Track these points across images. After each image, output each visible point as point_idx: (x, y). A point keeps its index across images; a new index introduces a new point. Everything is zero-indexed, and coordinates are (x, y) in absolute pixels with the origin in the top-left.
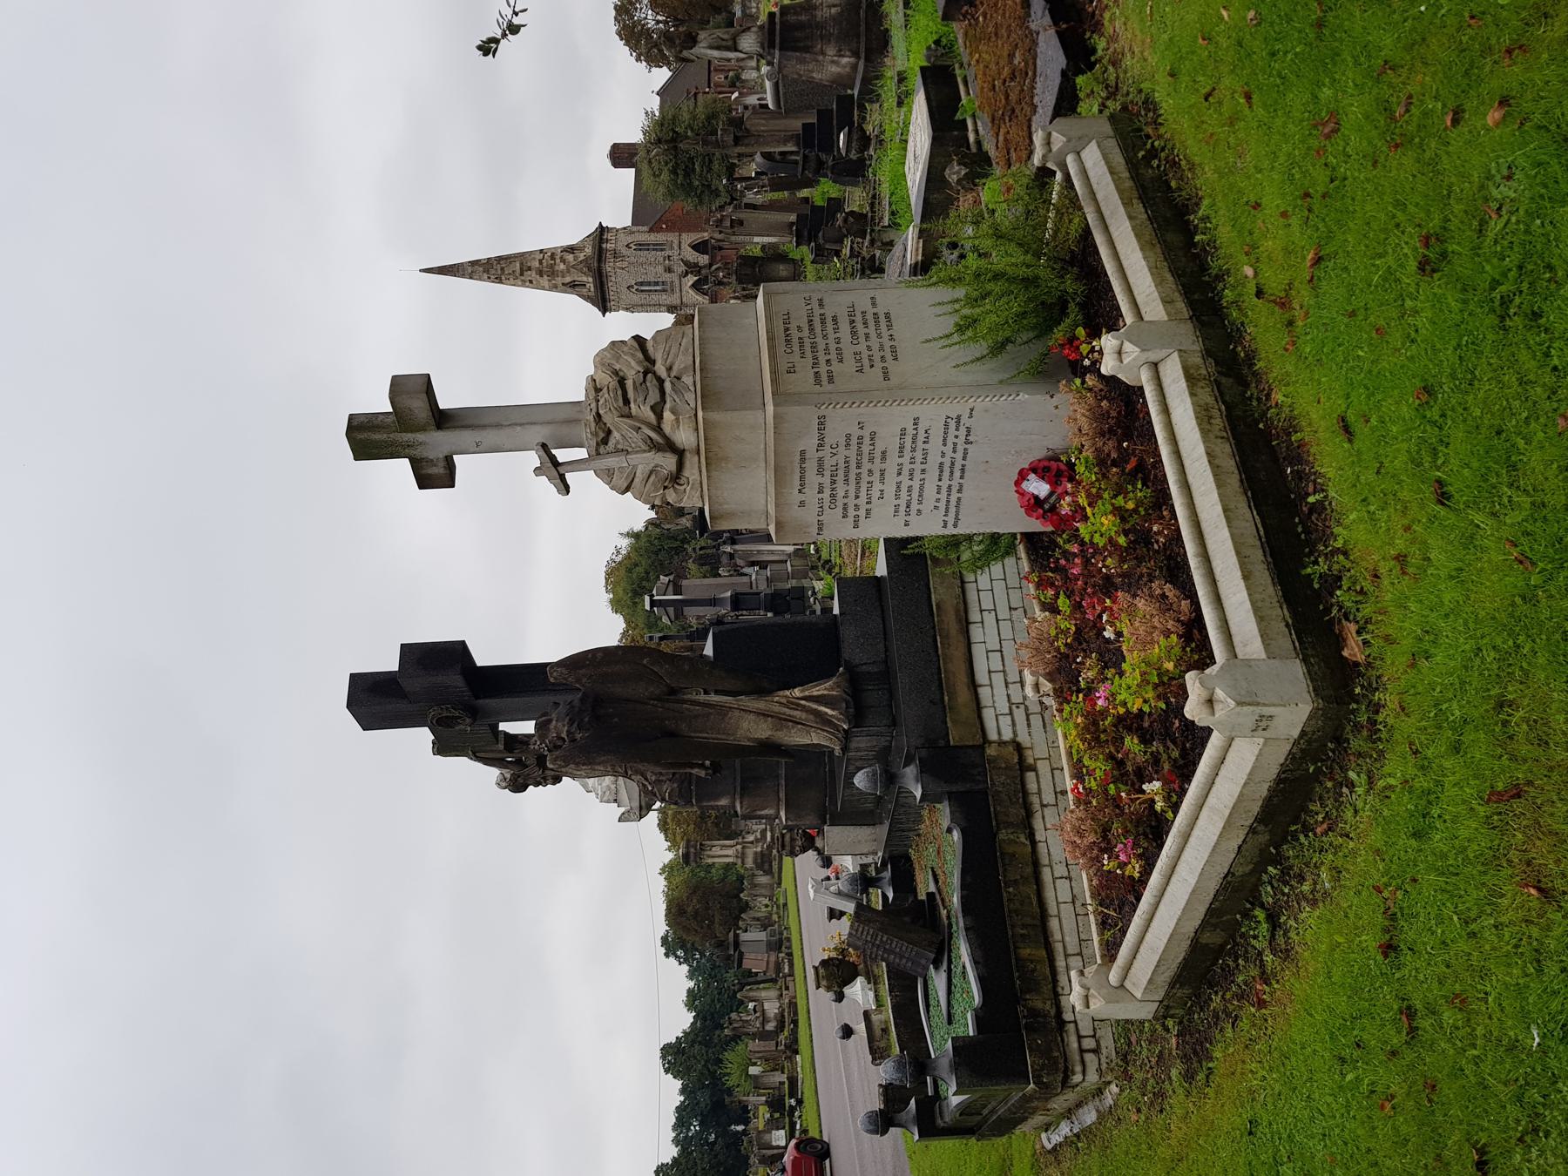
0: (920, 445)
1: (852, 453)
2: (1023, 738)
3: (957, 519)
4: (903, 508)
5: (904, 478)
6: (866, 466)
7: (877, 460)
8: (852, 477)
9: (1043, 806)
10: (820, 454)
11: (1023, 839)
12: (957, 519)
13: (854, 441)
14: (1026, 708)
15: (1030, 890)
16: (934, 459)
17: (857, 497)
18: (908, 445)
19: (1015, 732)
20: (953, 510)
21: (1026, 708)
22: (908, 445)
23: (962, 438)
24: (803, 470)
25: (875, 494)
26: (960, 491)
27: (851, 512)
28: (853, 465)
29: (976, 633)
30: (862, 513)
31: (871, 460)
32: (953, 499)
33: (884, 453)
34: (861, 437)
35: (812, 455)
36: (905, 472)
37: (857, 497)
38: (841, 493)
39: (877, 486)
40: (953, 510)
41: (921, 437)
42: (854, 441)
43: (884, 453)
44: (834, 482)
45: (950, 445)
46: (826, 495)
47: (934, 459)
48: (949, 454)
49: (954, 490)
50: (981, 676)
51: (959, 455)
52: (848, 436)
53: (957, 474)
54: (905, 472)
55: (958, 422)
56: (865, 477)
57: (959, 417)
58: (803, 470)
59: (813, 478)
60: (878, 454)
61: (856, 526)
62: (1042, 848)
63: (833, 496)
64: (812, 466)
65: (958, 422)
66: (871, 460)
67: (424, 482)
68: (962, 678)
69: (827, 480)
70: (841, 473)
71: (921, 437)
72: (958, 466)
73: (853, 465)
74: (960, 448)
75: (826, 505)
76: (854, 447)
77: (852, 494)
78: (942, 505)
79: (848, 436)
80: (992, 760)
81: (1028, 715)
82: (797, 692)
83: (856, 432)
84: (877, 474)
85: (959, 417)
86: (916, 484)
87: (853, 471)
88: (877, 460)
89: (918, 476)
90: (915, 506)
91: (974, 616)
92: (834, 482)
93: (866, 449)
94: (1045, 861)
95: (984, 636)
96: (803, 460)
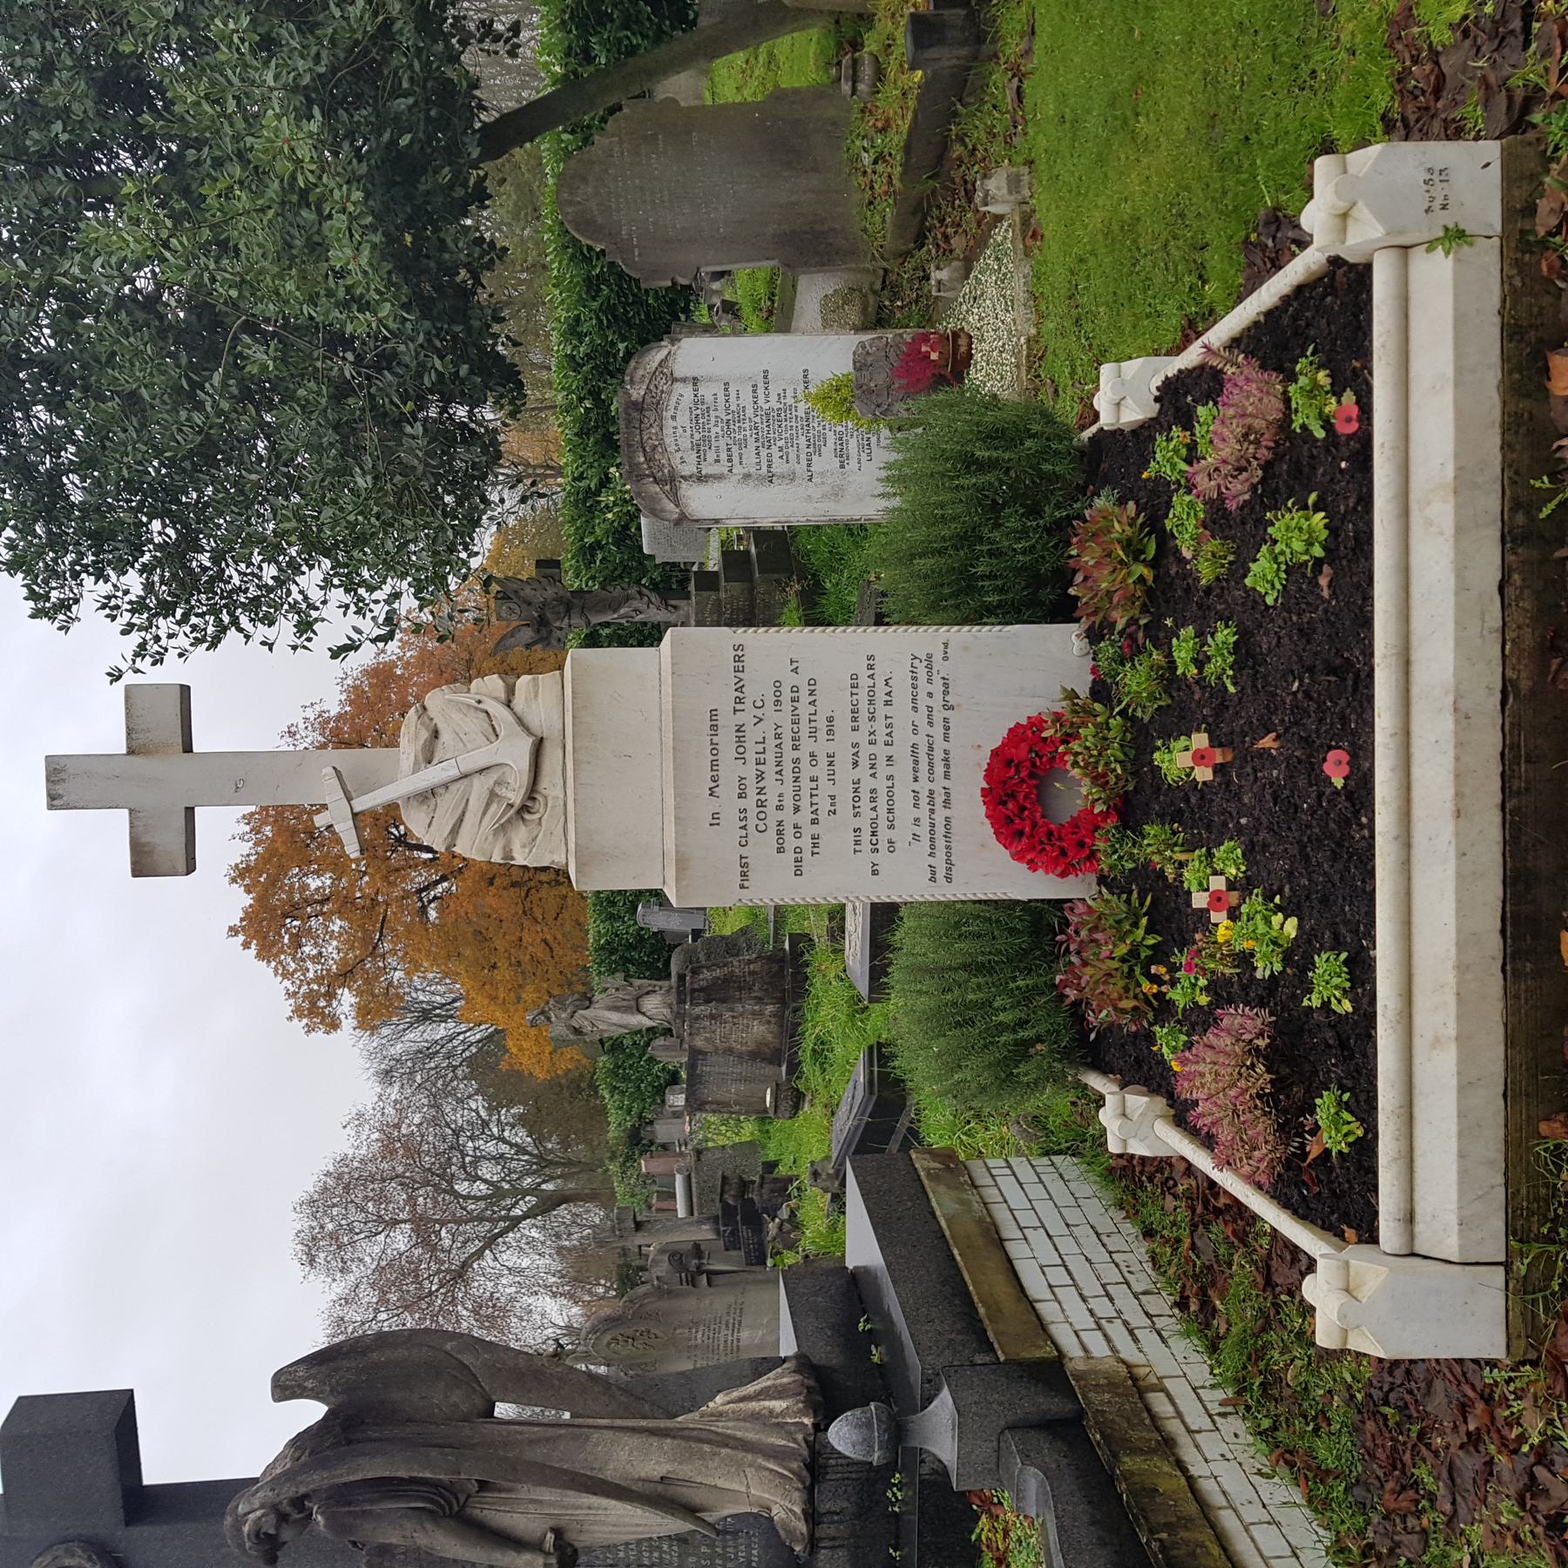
0: (882, 711)
1: (785, 719)
2: (1128, 1351)
3: (950, 864)
4: (866, 836)
5: (863, 772)
6: (807, 745)
7: (822, 735)
8: (788, 766)
9: (1189, 1431)
10: (740, 718)
11: (1166, 1468)
12: (950, 864)
13: (787, 695)
14: (1126, 1323)
15: (1205, 1536)
16: (904, 739)
17: (797, 809)
18: (864, 707)
19: (1113, 1349)
20: (941, 843)
21: (1126, 1323)
22: (864, 707)
23: (938, 696)
24: (714, 747)
25: (824, 805)
26: (947, 803)
27: (790, 842)
28: (787, 743)
29: (1016, 1250)
30: (806, 843)
31: (813, 734)
32: (938, 755)
33: (830, 720)
34: (795, 689)
35: (728, 721)
36: (864, 761)
37: (797, 809)
38: (772, 802)
39: (825, 787)
40: (941, 843)
41: (881, 697)
42: (787, 695)
43: (830, 720)
44: (760, 776)
45: (923, 710)
46: (750, 803)
47: (904, 739)
48: (924, 728)
49: (939, 800)
50: (1035, 1285)
51: (938, 731)
52: (778, 684)
53: (939, 769)
54: (864, 761)
55: (929, 667)
56: (807, 771)
57: (929, 656)
58: (714, 747)
59: (730, 770)
60: (822, 724)
61: (798, 873)
62: (1208, 1487)
63: (761, 804)
64: (727, 739)
65: (929, 667)
66: (813, 734)
67: (143, 864)
68: (1003, 1290)
69: (750, 771)
70: (770, 757)
71: (881, 697)
72: (938, 755)
73: (787, 743)
74: (938, 717)
75: (752, 822)
76: (787, 706)
77: (789, 803)
78: (924, 830)
79: (778, 684)
80: (1079, 1376)
81: (1131, 1332)
82: (719, 1399)
83: (789, 680)
84: (823, 761)
85: (929, 656)
86: (881, 785)
87: (788, 755)
88: (822, 735)
89: (883, 769)
90: (884, 834)
91: (1009, 1231)
92: (760, 776)
93: (804, 710)
94: (1218, 1500)
95: (1033, 1262)
96: (714, 727)
